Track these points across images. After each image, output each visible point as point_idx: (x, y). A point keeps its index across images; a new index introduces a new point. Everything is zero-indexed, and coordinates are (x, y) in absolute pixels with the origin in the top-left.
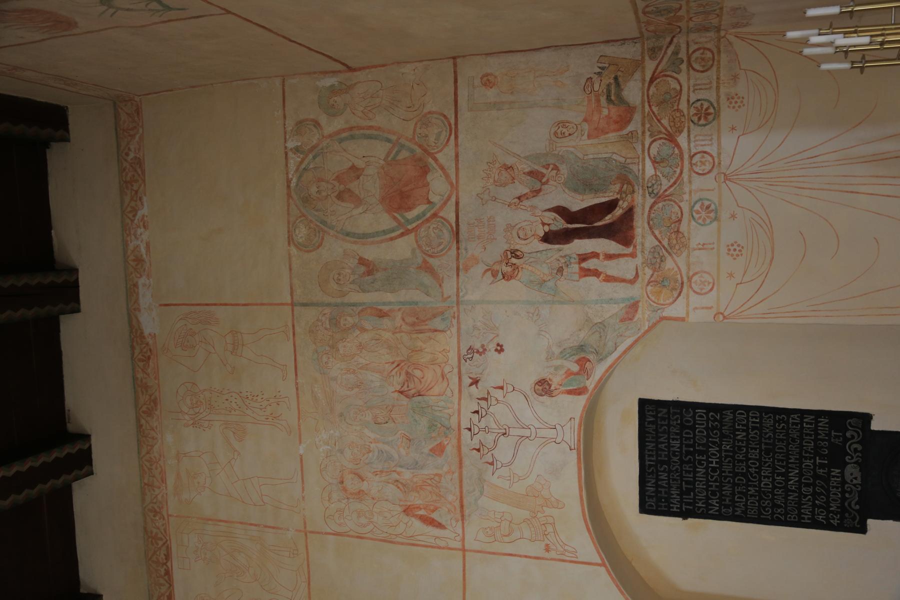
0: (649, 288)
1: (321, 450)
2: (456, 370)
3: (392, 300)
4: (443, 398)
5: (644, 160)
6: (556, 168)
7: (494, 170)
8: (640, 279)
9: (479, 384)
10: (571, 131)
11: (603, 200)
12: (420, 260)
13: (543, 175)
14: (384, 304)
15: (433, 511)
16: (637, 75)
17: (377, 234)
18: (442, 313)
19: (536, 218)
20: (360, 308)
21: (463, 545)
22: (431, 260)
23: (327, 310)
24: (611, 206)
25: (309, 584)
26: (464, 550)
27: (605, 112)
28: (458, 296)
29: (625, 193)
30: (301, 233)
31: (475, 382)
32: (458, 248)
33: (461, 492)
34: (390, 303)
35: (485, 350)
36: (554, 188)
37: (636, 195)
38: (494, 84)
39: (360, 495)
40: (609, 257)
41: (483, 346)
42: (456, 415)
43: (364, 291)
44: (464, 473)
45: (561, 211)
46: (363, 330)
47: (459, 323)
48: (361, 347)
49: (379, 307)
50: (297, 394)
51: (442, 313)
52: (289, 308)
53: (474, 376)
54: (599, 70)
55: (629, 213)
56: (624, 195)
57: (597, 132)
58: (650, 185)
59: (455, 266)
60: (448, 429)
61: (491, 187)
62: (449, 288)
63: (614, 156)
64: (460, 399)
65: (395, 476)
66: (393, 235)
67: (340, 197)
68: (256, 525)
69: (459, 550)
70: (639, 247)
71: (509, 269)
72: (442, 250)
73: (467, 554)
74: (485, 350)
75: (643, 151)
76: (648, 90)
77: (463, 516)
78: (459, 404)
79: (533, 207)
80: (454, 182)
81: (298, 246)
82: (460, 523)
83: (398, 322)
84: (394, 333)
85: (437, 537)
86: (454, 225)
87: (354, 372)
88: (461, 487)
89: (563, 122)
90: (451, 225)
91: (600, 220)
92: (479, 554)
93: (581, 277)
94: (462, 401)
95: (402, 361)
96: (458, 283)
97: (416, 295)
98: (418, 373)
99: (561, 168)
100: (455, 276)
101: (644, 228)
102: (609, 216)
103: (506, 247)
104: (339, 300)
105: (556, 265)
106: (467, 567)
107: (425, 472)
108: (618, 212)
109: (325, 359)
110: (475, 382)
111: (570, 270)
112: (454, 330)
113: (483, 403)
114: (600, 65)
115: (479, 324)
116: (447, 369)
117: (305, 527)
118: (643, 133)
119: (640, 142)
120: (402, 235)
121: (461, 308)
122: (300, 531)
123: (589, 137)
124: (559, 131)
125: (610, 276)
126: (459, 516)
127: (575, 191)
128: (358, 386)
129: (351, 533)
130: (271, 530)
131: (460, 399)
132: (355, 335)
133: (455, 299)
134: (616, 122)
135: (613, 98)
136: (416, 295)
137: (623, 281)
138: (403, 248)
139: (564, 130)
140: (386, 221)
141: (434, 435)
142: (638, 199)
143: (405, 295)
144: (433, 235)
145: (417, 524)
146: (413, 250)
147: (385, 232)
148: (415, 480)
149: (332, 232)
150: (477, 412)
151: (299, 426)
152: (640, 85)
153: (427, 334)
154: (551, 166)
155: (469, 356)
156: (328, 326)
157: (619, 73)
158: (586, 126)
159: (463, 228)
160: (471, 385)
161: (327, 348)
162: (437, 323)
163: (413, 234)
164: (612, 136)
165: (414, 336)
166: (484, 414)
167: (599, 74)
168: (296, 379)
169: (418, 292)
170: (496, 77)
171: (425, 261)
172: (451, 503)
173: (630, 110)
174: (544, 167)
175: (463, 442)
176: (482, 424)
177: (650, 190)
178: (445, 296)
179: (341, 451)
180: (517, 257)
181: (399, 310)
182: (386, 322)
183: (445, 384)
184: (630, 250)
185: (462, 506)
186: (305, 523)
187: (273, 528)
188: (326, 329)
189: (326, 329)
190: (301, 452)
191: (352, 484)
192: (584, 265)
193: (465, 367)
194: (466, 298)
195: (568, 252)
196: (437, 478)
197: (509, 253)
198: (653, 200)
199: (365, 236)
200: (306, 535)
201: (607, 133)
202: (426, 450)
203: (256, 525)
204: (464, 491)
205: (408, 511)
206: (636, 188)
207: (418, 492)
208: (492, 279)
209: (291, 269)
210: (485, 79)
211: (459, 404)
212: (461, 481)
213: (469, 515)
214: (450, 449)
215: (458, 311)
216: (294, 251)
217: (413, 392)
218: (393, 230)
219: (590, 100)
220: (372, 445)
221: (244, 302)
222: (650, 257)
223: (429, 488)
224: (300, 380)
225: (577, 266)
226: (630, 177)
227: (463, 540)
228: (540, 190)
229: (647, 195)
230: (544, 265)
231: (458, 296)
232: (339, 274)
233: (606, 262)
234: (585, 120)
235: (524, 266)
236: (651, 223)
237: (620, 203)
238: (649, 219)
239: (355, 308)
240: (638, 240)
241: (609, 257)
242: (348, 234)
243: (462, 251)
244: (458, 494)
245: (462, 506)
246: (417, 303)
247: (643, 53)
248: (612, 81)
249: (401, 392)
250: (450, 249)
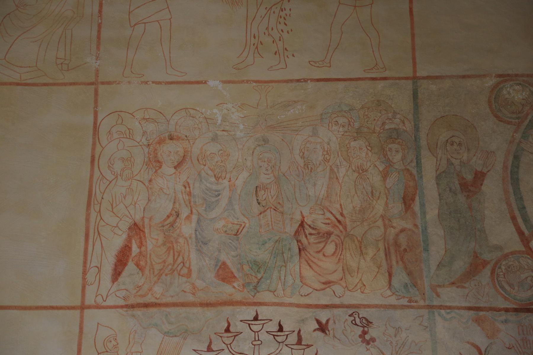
1: (215, 111)
2: (337, 301)
3: (428, 217)
4: (298, 281)
9: (320, 334)
12: (487, 256)
14: (422, 205)
15: (137, 265)
17: (520, 199)
18: (415, 285)
20: (414, 172)
21: (89, 307)
22: (487, 271)
23: (409, 126)
25: (18, 84)
26: (83, 307)
28: (441, 307)
30: (516, 94)
31: (322, 328)
32: (507, 310)
33: (167, 305)
34: (424, 213)
35: (368, 343)
39: (155, 162)
41: (373, 340)
42: (276, 301)
43: (438, 178)
44: (195, 310)
46: (385, 175)
47: (403, 307)
48: (361, 171)
49: (417, 198)
50: (291, 81)
51: (415, 285)
52: (411, 75)
53: (330, 326)
59: (482, 305)
60: (255, 288)
62: (451, 296)
64: (298, 306)
65: (185, 213)
66: (520, 220)
68: (100, 11)
69: (83, 302)
72: (502, 287)
73: (77, 312)
74: (368, 343)
77: (133, 306)
78: (291, 305)
81: (496, 89)
82: (122, 302)
83: (399, 224)
84: (383, 217)
85: (99, 269)
87: (326, 160)
88: (175, 305)
92: (77, 330)
94: (296, 309)
95: (345, 228)
96: (459, 308)
97: (438, 249)
98: (330, 248)
100: (468, 305)
104: (423, 142)
106: (56, 311)
107: (193, 255)
109: (341, 120)
110: (322, 328)
112: (393, 300)
113: (293, 338)
115: (404, 335)
116: (338, 289)
117: (103, 83)
120: (521, 233)
121: (425, 312)
122: (97, 75)
126: (132, 301)
128: (306, 165)
129: (98, 149)
130: (95, 33)
131: (298, 306)
132: (377, 163)
133: (435, 303)
136: (438, 249)
141: (246, 268)
143: (436, 233)
144: (523, 276)
145: (118, 242)
146: (498, 248)
147: (522, 209)
148: (181, 240)
149: (518, 136)
150: (281, 329)
151: (248, 81)
153: (384, 263)
155: (358, 321)
156: (387, 127)
160: (319, 322)
161: (357, 125)
162: (400, 277)
163: (524, 249)
165: (381, 245)
166: (279, 339)
168: (312, 80)
169: (443, 252)
171: (485, 263)
172: (150, 290)
175: (238, 309)
176: (263, 336)
178: (439, 290)
179: (215, 139)
181: (416, 225)
182: (397, 207)
183: (317, 286)
185: (146, 305)
186: (109, 83)
187: (99, 37)
188: (384, 124)
189: (384, 124)
190: (211, 83)
191: (170, 152)
193: (342, 314)
194: (438, 319)
196: (185, 271)
199: (516, 182)
200: (92, 84)
202: (223, 257)
203: (100, 11)
204: (168, 309)
205: (136, 229)
207: (164, 244)
209: (464, 77)
211: (291, 305)
212: (183, 305)
213: (133, 316)
214: (227, 290)
215: (420, 307)
216: (490, 82)
217: (304, 240)
218: (526, 220)
220: (226, 182)
221: (414, 10)
223: (170, 260)
224: (310, 85)
227: (98, 307)
231: (441, 307)
232: (460, 144)
239: (414, 164)
242: (516, 158)
243: (503, 316)
244: (164, 300)
245: (146, 305)
246: (426, 250)
249: (302, 224)
250: (506, 299)
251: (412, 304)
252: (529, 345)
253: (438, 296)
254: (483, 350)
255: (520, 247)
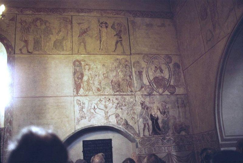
6: (166, 117)
13: (165, 115)
16: (186, 134)
19: (156, 113)
40: (149, 129)
65: (90, 79)
67: (156, 67)
108: (158, 131)
120: (149, 82)
138: (146, 81)
140: (152, 78)
150: (110, 99)
173: (179, 133)
255: (149, 84)
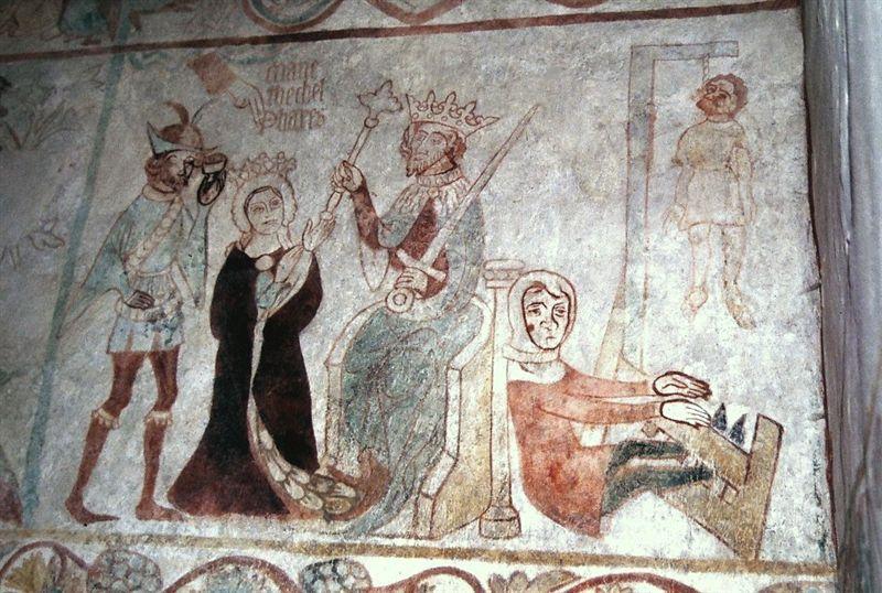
0: (47, 554)
5: (422, 553)
7: (451, 122)
8: (78, 527)
10: (540, 333)
11: (318, 426)
13: (416, 254)
16: (706, 546)
24: (299, 449)
27: (591, 437)
28: (138, 47)
29: (331, 490)
32: (255, 41)
36: (375, 283)
37: (319, 523)
38: (709, 113)
45: (308, 301)
54: (731, 421)
55: (269, 503)
56: (322, 488)
57: (528, 409)
58: (341, 569)
59: (210, 36)
61: (404, 114)
63: (446, 461)
70: (164, 527)
71: (175, 171)
75: (450, 553)
76: (652, 580)
79: (330, 229)
80: (436, 21)
86: (319, 28)
89: (573, 306)
90: (312, 23)
91: (261, 413)
93: (117, 357)
99: (429, 302)
100: (186, 38)
101: (219, 544)
102: (267, 439)
103: (236, 160)
105: (159, 291)
108: (276, 469)
111: (140, 327)
114: (749, 426)
118: (512, 557)
119: (479, 543)
121: (108, 57)
123: (516, 387)
124: (543, 296)
125: (103, 438)
127: (359, 344)
134: (553, 472)
135: (635, 462)
137: (83, 479)
139: (545, 313)
142: (306, 532)
152: (674, 554)
154: (441, 276)
157: (716, 486)
158: (553, 375)
159: (304, 51)
164: (510, 459)
167: (720, 420)
170: (731, 115)
173: (590, 520)
174: (443, 254)
177: (327, 571)
180: (203, 189)
184: (162, 501)
192: (148, 365)
195: (189, 324)
197: (218, 167)
198: (294, 576)
201: (522, 442)
206: (341, 526)
208: (160, 126)
210: (729, 87)
219: (633, 389)
222: (132, 561)
225: (147, 346)
226: (375, 510)
228: (375, 246)
229: (311, 560)
230: (167, 259)
231: (138, 47)
233: (141, 428)
234: (570, 374)
235: (177, 206)
236: (230, 568)
237: (303, 477)
238: (241, 563)
240: (190, 526)
241: (154, 439)
247: (784, 566)
248: (691, 462)
251: (90, 47)
252: (279, 100)
253: (139, 28)
254: (191, 113)
